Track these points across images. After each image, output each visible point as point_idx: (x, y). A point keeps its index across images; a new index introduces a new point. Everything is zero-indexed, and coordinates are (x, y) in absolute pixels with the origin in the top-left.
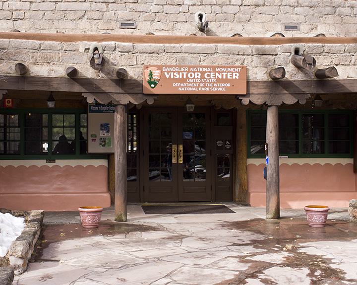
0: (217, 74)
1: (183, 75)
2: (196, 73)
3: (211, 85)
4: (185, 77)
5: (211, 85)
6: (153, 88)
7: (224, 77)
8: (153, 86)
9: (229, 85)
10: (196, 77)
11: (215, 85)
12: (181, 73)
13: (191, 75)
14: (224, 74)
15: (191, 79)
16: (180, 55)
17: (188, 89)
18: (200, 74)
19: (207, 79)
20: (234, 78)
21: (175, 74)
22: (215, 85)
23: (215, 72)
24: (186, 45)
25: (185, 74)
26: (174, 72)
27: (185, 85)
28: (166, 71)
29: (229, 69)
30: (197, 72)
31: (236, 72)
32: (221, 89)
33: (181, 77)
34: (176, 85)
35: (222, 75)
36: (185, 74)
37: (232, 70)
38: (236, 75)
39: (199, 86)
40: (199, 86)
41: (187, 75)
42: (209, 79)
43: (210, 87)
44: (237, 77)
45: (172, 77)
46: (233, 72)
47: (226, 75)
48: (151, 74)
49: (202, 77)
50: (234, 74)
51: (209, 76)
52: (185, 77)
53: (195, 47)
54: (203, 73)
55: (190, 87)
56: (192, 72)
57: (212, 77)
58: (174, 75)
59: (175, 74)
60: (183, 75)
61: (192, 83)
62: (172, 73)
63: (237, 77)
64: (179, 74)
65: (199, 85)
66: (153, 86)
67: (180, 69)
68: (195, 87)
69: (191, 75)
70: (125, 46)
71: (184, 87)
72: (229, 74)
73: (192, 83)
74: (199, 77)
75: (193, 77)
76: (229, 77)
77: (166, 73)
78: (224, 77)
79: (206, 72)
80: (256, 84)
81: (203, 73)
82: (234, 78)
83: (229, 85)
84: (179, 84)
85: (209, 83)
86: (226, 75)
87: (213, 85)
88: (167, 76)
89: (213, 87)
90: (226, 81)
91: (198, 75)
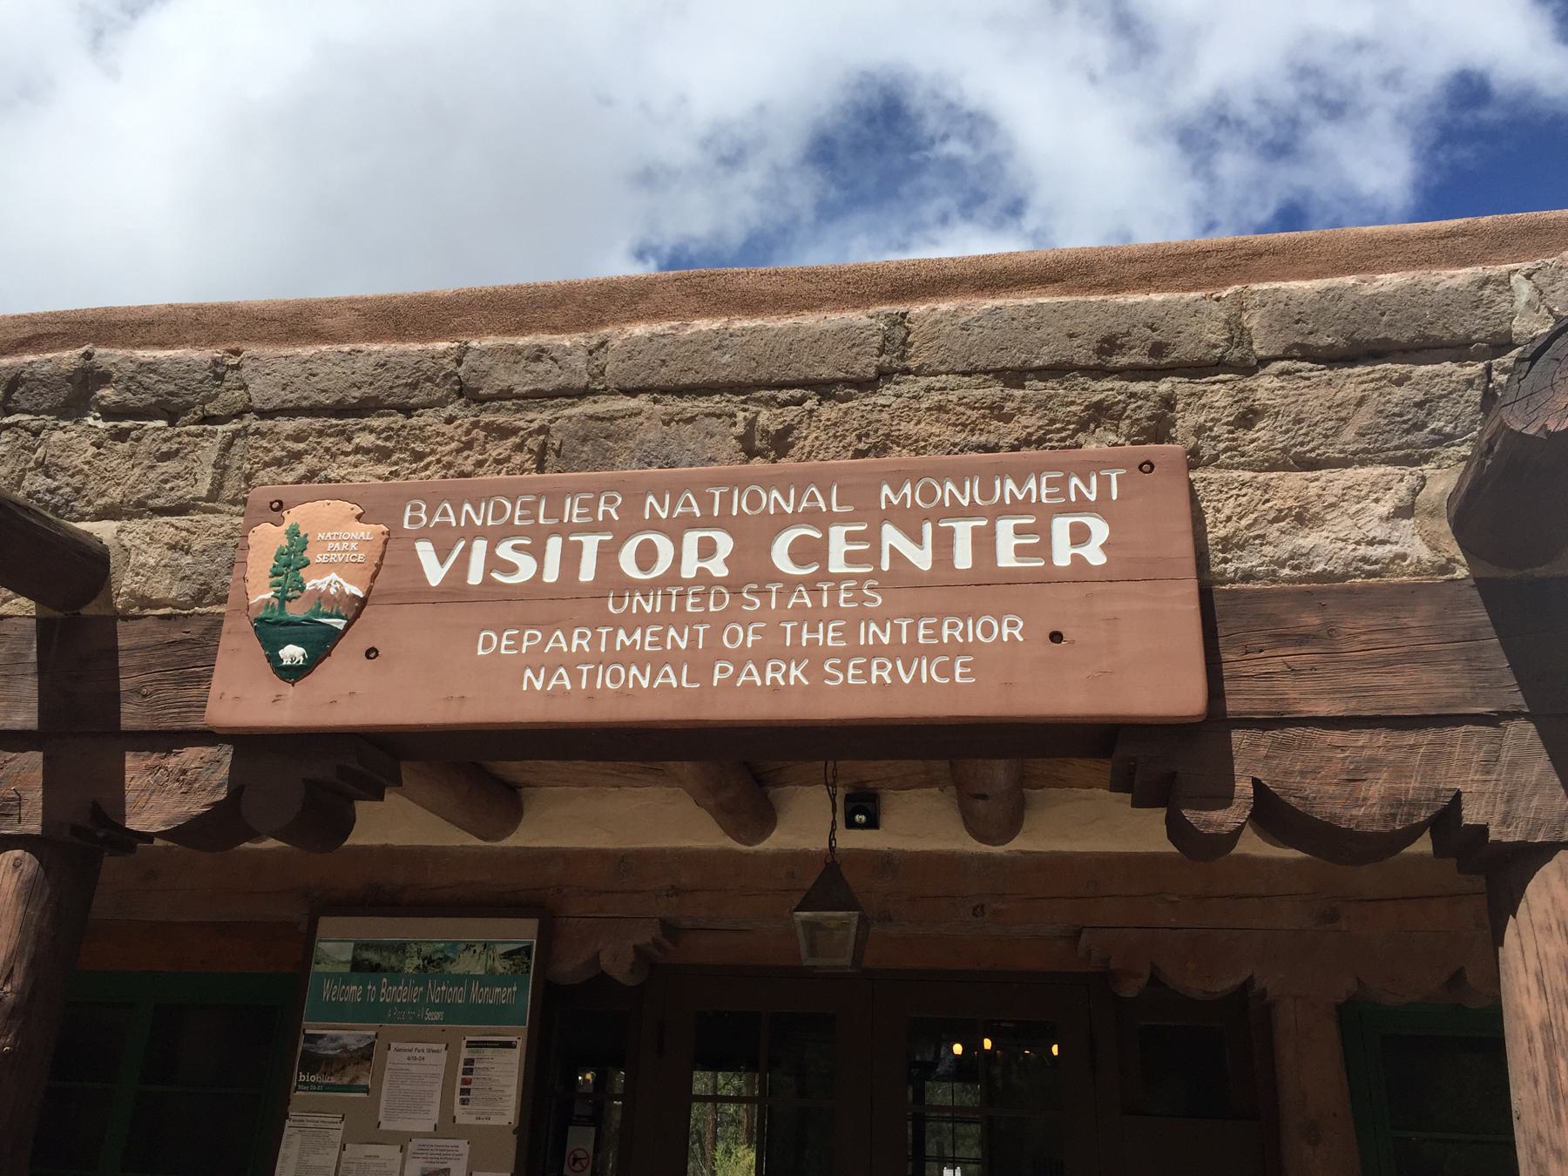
0: (891, 536)
1: (571, 556)
2: (691, 539)
3: (828, 636)
4: (587, 573)
5: (828, 636)
6: (292, 674)
7: (963, 558)
8: (292, 653)
9: (1008, 630)
10: (689, 570)
11: (871, 632)
12: (554, 545)
13: (647, 556)
14: (963, 531)
15: (646, 588)
16: (587, 407)
17: (604, 680)
18: (725, 543)
19: (791, 583)
20: (1062, 555)
21: (505, 551)
22: (871, 632)
23: (872, 517)
24: (640, 330)
25: (590, 543)
26: (495, 537)
27: (579, 641)
28: (423, 535)
29: (1008, 488)
30: (707, 522)
31: (1082, 506)
32: (927, 671)
33: (551, 575)
34: (504, 643)
35: (944, 542)
36: (590, 543)
37: (1038, 489)
38: (1080, 535)
39: (716, 652)
40: (716, 652)
41: (608, 554)
42: (812, 585)
43: (814, 657)
44: (1094, 555)
45: (475, 577)
46: (1045, 514)
47: (984, 543)
48: (291, 562)
49: (750, 569)
50: (1061, 527)
51: (805, 552)
52: (587, 573)
53: (719, 342)
54: (753, 537)
55: (631, 657)
56: (656, 525)
57: (837, 565)
58: (493, 563)
59: (505, 551)
60: (571, 556)
61: (643, 620)
62: (480, 547)
63: (1094, 555)
64: (538, 553)
65: (713, 636)
66: (292, 653)
67: (555, 510)
68: (674, 658)
69: (647, 556)
70: (150, 367)
71: (571, 663)
72: (1005, 527)
73: (643, 620)
74: (717, 568)
75: (660, 569)
76: (1006, 558)
77: (425, 551)
78: (963, 558)
79: (782, 522)
80: (1311, 620)
81: (753, 537)
82: (1062, 555)
83: (1008, 630)
84: (531, 638)
85: (814, 618)
86: (984, 543)
87: (850, 632)
88: (435, 573)
89: (845, 656)
90: (988, 585)
91: (707, 549)
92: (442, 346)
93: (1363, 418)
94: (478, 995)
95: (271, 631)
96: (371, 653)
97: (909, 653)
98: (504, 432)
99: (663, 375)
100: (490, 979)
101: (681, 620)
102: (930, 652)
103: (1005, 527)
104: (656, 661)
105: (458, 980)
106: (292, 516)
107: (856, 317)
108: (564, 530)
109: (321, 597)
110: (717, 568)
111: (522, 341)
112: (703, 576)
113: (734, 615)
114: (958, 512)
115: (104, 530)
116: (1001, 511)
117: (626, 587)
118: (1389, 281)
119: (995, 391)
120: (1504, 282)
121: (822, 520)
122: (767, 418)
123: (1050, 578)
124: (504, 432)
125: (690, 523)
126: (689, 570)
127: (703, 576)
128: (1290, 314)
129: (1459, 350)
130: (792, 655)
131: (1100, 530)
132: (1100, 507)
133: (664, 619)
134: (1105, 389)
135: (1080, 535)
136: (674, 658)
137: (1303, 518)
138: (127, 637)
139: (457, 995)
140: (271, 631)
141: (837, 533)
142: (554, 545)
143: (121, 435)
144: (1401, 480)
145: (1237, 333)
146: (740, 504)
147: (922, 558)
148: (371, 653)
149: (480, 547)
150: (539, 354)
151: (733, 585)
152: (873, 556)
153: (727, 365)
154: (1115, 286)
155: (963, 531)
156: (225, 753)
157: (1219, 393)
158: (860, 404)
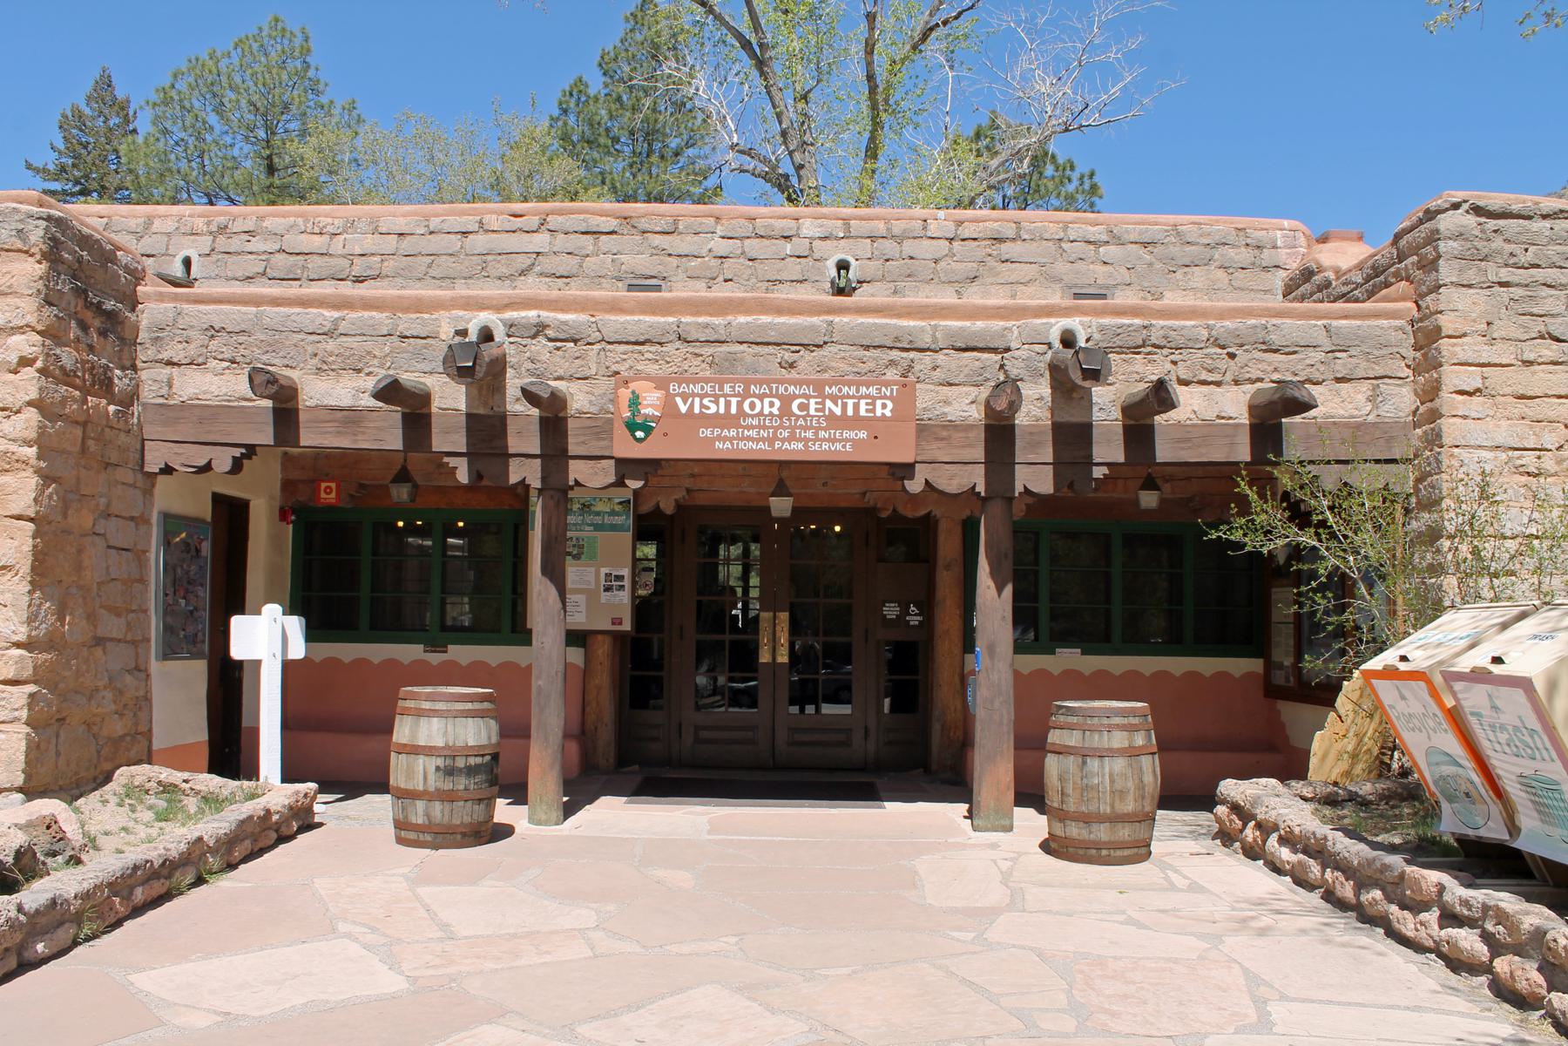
0: (829, 403)
1: (728, 404)
2: (767, 401)
3: (810, 434)
4: (734, 410)
5: (810, 434)
6: (640, 440)
7: (850, 412)
8: (639, 434)
9: (863, 435)
10: (766, 411)
11: (822, 434)
12: (722, 400)
13: (752, 406)
14: (850, 402)
15: (753, 416)
16: (724, 348)
17: (741, 445)
18: (777, 403)
19: (798, 417)
20: (879, 413)
21: (706, 401)
22: (822, 434)
23: (823, 397)
24: (742, 319)
25: (734, 401)
26: (702, 397)
27: (733, 433)
28: (678, 395)
29: (863, 390)
30: (771, 396)
31: (885, 397)
32: (839, 446)
33: (722, 411)
34: (708, 433)
35: (844, 406)
36: (734, 401)
37: (873, 391)
38: (884, 406)
39: (775, 438)
40: (775, 438)
41: (740, 404)
42: (804, 417)
43: (806, 440)
44: (888, 413)
45: (697, 410)
46: (874, 399)
47: (856, 407)
48: (635, 402)
49: (785, 411)
50: (879, 403)
51: (803, 407)
52: (734, 410)
53: (771, 326)
54: (786, 400)
55: (749, 439)
56: (755, 395)
57: (812, 412)
58: (702, 406)
59: (706, 401)
60: (728, 404)
61: (753, 427)
62: (697, 400)
63: (888, 413)
64: (717, 403)
65: (775, 433)
66: (639, 434)
67: (721, 389)
68: (763, 440)
69: (752, 406)
70: (565, 323)
71: (731, 440)
72: (863, 402)
73: (753, 427)
74: (776, 411)
75: (757, 410)
76: (863, 413)
77: (679, 400)
78: (850, 412)
79: (795, 397)
80: (945, 434)
81: (786, 400)
82: (879, 413)
83: (863, 435)
84: (717, 431)
85: (806, 428)
86: (856, 407)
87: (816, 434)
88: (683, 409)
89: (815, 441)
90: (856, 422)
91: (772, 405)
92: (671, 319)
93: (966, 371)
94: (607, 520)
95: (632, 427)
96: (665, 435)
97: (833, 441)
98: (697, 355)
99: (752, 338)
100: (613, 513)
101: (765, 427)
102: (839, 441)
103: (863, 402)
104: (758, 440)
105: (598, 514)
106: (632, 386)
107: (815, 320)
108: (725, 396)
109: (646, 416)
110: (776, 411)
111: (701, 320)
112: (771, 414)
113: (781, 426)
114: (849, 397)
115: (561, 385)
116: (862, 397)
117: (746, 415)
118: (980, 324)
119: (863, 353)
120: (1010, 329)
121: (808, 397)
122: (789, 357)
123: (875, 419)
124: (697, 355)
125: (765, 395)
126: (766, 411)
127: (771, 414)
128: (950, 334)
129: (994, 350)
130: (800, 440)
131: (890, 405)
132: (891, 398)
133: (759, 427)
134: (895, 354)
135: (884, 406)
136: (763, 440)
137: (947, 402)
138: (571, 424)
139: (598, 520)
140: (632, 427)
141: (812, 401)
142: (722, 400)
143: (558, 349)
144: (974, 391)
145: (935, 339)
146: (781, 390)
147: (838, 411)
148: (665, 435)
149: (697, 400)
150: (707, 326)
151: (780, 417)
152: (822, 410)
153: (772, 336)
154: (899, 316)
155: (850, 402)
156: (612, 462)
157: (927, 358)
158: (818, 353)
